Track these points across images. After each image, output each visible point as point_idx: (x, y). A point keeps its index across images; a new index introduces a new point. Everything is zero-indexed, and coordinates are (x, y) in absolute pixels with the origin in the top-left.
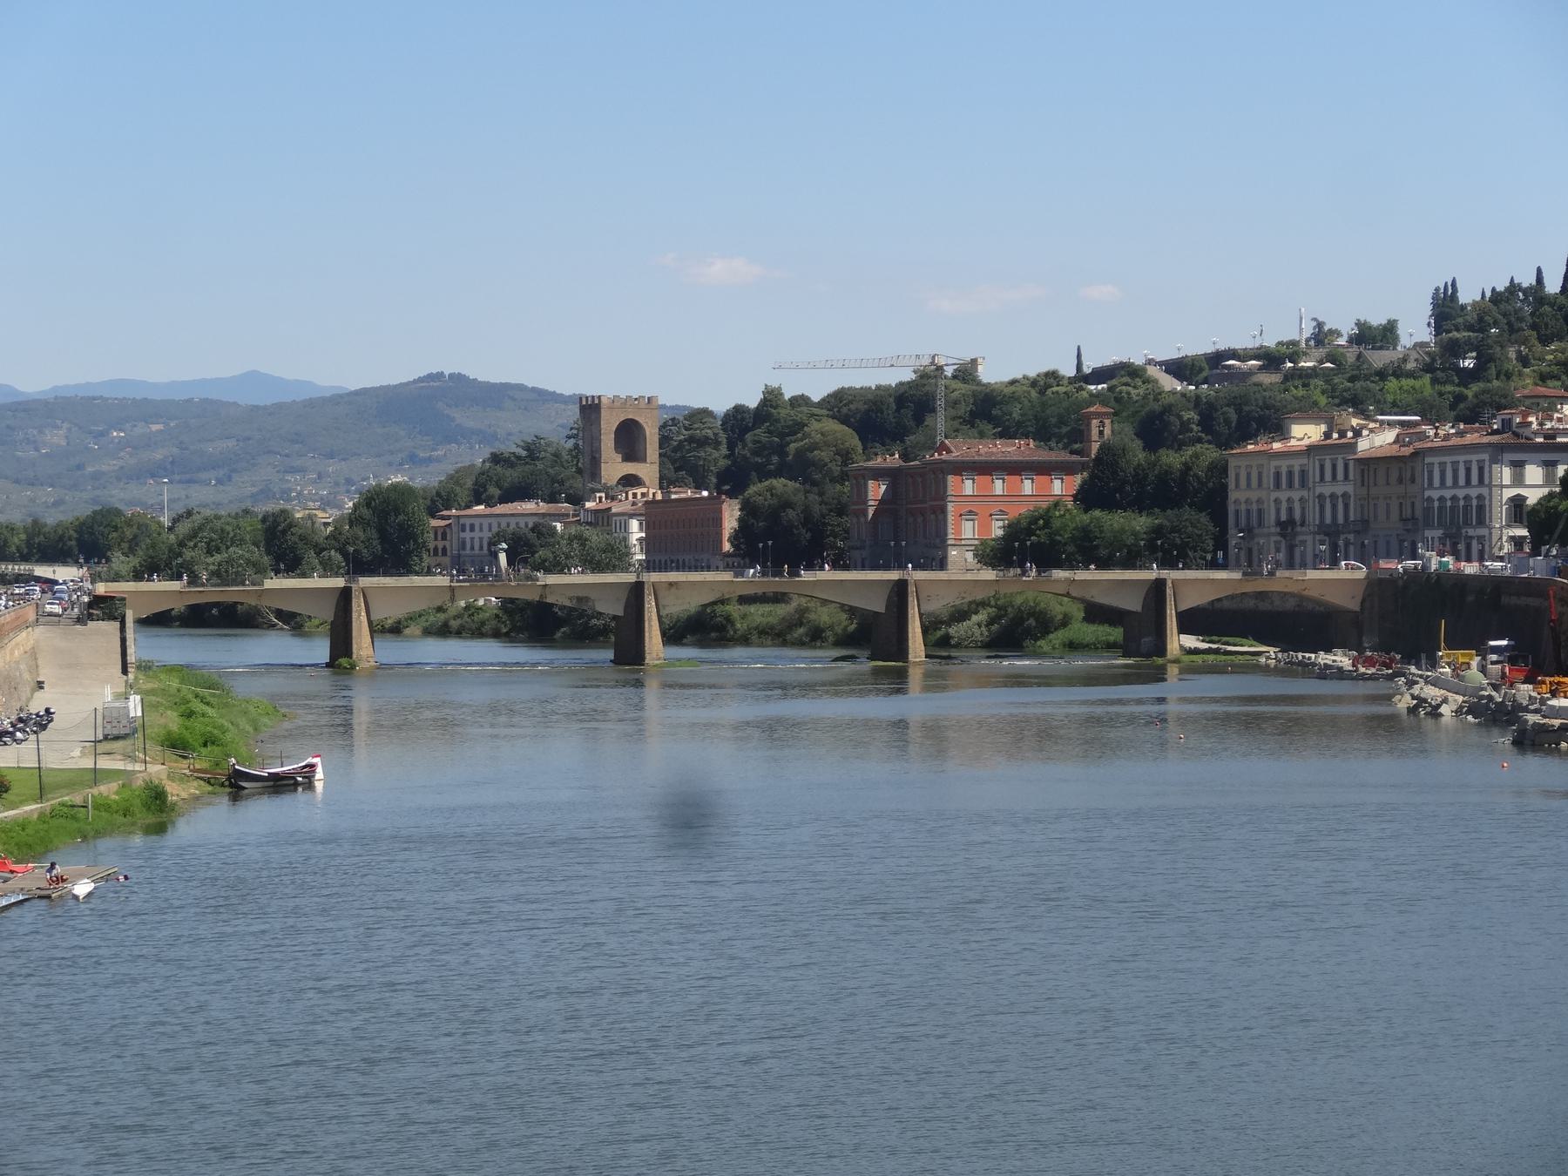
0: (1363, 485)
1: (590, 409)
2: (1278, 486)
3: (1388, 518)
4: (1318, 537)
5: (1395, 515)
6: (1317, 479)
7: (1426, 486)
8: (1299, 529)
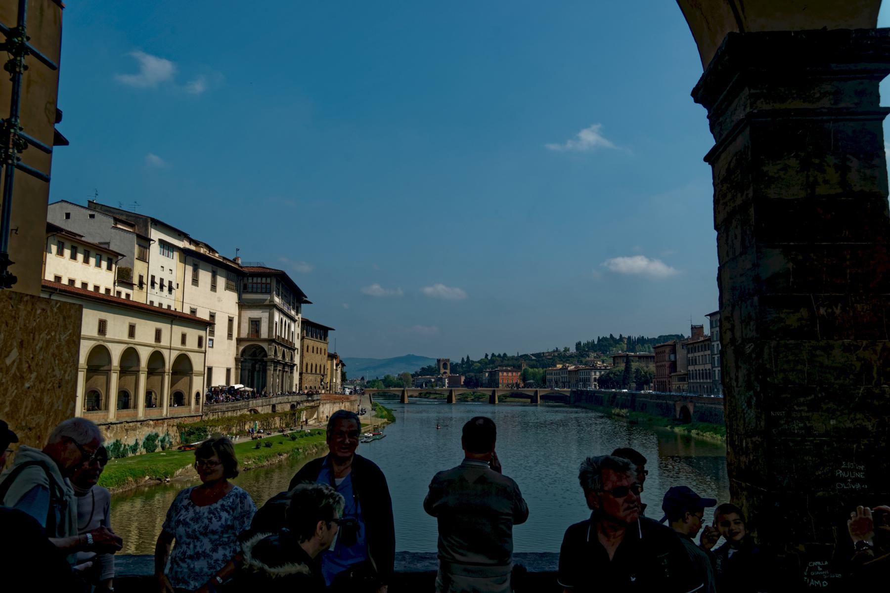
1: (439, 361)
2: (555, 375)
5: (574, 380)
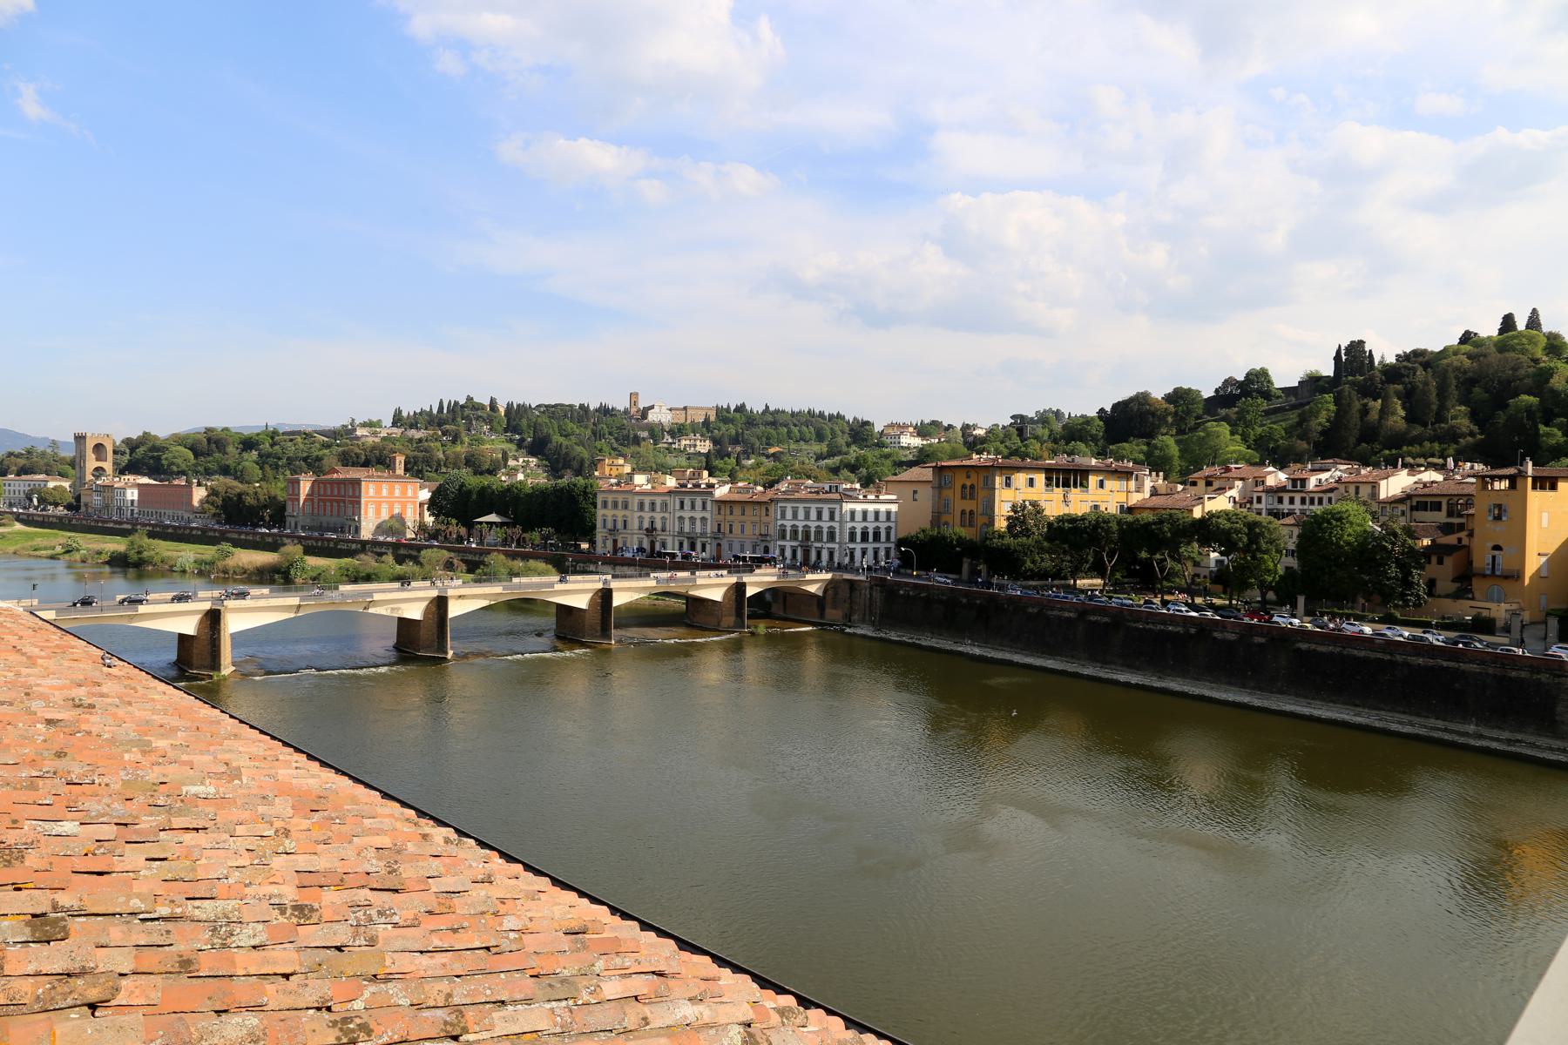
0: (719, 514)
1: (80, 439)
3: (743, 531)
4: (676, 538)
6: (678, 507)
7: (779, 518)
8: (658, 533)
